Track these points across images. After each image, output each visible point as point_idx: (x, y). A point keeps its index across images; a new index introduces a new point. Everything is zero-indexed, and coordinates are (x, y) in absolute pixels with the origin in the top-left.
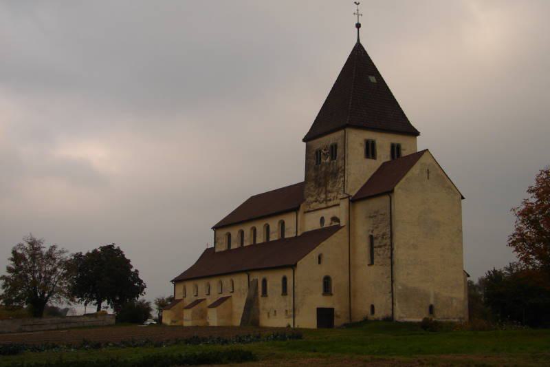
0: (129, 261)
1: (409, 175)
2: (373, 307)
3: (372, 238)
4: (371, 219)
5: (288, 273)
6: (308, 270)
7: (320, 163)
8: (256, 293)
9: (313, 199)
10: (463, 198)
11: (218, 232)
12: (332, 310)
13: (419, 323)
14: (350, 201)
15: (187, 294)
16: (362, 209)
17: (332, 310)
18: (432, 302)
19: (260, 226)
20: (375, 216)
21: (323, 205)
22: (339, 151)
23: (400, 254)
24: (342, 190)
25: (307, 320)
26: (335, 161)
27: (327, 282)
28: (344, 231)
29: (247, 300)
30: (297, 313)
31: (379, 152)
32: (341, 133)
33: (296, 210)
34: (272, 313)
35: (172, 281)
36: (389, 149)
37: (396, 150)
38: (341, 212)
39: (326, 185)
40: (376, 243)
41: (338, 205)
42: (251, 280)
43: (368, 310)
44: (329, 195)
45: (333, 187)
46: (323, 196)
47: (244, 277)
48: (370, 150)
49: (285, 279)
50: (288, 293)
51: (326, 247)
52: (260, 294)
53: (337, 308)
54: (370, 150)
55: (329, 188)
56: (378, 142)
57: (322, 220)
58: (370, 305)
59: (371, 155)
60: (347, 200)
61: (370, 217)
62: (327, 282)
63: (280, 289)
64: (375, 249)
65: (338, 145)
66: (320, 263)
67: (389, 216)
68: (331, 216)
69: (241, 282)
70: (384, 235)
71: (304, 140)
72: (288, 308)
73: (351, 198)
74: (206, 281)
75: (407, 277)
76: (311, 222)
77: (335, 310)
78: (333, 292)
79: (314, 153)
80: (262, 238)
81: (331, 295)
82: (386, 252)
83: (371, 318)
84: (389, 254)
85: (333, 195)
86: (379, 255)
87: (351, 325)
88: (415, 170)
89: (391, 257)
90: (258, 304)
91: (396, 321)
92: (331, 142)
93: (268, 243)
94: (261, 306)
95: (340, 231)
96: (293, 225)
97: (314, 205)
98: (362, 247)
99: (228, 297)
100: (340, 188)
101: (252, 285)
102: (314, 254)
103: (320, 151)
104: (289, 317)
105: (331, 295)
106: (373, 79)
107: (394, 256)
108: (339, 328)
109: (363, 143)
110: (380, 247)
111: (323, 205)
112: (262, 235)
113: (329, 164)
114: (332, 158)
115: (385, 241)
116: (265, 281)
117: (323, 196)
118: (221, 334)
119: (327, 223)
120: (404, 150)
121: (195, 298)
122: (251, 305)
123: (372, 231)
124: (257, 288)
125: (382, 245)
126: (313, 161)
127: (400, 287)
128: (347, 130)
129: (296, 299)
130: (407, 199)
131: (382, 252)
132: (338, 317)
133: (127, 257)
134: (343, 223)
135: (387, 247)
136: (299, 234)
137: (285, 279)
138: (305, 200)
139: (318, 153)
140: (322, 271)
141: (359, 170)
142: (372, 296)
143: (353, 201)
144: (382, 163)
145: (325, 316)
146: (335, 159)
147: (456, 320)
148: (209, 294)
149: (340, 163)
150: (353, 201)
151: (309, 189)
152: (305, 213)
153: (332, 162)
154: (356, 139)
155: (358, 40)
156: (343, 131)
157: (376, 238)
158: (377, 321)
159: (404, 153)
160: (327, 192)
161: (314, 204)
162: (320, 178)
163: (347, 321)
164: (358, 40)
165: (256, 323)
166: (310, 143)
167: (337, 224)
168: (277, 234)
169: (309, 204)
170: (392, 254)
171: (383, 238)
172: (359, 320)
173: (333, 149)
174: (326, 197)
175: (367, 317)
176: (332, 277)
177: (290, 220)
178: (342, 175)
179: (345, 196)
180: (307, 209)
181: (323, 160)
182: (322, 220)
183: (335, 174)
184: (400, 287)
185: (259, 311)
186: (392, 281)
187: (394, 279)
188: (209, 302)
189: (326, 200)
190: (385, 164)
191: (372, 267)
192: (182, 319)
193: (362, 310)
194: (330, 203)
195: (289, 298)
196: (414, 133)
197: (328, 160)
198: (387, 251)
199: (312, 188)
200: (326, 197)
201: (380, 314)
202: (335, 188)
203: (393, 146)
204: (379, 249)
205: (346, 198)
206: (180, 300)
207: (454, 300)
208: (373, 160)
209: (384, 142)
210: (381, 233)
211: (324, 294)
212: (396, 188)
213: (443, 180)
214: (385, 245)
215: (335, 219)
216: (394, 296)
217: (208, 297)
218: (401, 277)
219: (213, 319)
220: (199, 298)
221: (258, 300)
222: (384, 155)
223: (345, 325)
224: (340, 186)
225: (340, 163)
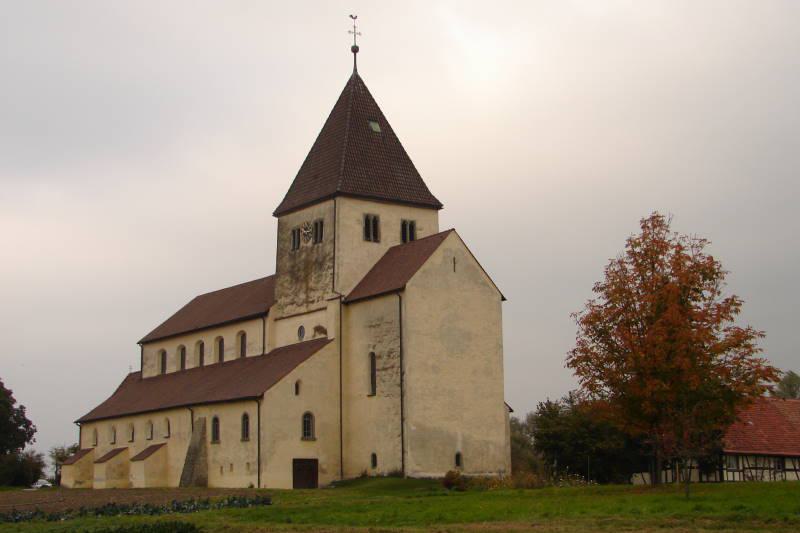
0: (10, 392)
1: (427, 266)
2: (374, 457)
3: (373, 356)
4: (373, 330)
5: (251, 409)
6: (281, 405)
7: (298, 248)
8: (203, 439)
9: (288, 300)
10: (503, 299)
11: (148, 348)
12: (315, 461)
13: (440, 479)
14: (342, 303)
15: (99, 440)
16: (357, 313)
17: (315, 461)
18: (459, 448)
19: (209, 340)
20: (379, 325)
21: (303, 309)
22: (327, 230)
23: (411, 378)
24: (331, 286)
25: (279, 477)
26: (320, 245)
27: (308, 421)
28: (333, 347)
29: (190, 447)
30: (263, 466)
31: (384, 232)
32: (329, 204)
34: (226, 469)
35: (76, 422)
36: (398, 228)
37: (408, 229)
38: (328, 318)
39: (306, 279)
40: (379, 364)
41: (325, 309)
42: (196, 419)
43: (368, 462)
44: (312, 294)
45: (318, 282)
46: (302, 296)
48: (371, 229)
49: (246, 418)
50: (251, 437)
51: (305, 371)
52: (209, 438)
53: (322, 460)
54: (371, 229)
55: (312, 284)
56: (382, 220)
57: (301, 331)
58: (370, 455)
59: (372, 237)
60: (338, 300)
61: (370, 326)
62: (308, 421)
63: (239, 434)
64: (377, 373)
66: (297, 393)
67: (398, 323)
68: (315, 324)
69: (181, 421)
71: (276, 214)
72: (250, 460)
73: (343, 299)
75: (424, 412)
76: (285, 335)
77: (320, 462)
78: (316, 436)
79: (290, 232)
80: (212, 357)
81: (314, 439)
82: (394, 377)
83: (372, 472)
84: (398, 381)
85: (318, 294)
86: (384, 381)
87: (343, 484)
88: (437, 258)
89: (401, 385)
90: (206, 455)
91: (408, 477)
92: (315, 218)
93: (221, 364)
94: (210, 457)
95: (327, 347)
96: (258, 339)
97: (290, 310)
98: (360, 369)
99: (162, 445)
100: (327, 285)
101: (197, 427)
102: (289, 381)
103: (299, 230)
104: (251, 474)
105: (314, 439)
106: (376, 127)
107: (404, 383)
108: (323, 488)
109: (362, 219)
110: (385, 369)
111: (303, 309)
112: (213, 352)
113: (312, 248)
114: (316, 242)
116: (216, 421)
117: (302, 296)
118: (151, 500)
119: (309, 335)
120: (421, 230)
121: (113, 447)
122: (195, 456)
123: (374, 347)
124: (204, 428)
125: (386, 368)
126: (289, 245)
127: (413, 428)
128: (339, 200)
129: (261, 446)
130: (425, 297)
131: (387, 377)
132: (324, 472)
133: (7, 386)
134: (332, 334)
135: (395, 369)
136: (267, 352)
137: (246, 418)
138: (276, 301)
139: (296, 233)
140: (300, 406)
141: (354, 258)
142: (373, 440)
143: (347, 303)
144: (388, 248)
145: (305, 471)
146: (321, 241)
147: (494, 474)
148: (132, 441)
150: (347, 303)
151: (282, 285)
152: (276, 320)
153: (316, 246)
154: (351, 214)
155: (355, 70)
156: (332, 202)
157: (380, 357)
158: (380, 477)
159: (420, 234)
160: (308, 290)
161: (290, 307)
162: (299, 270)
163: (338, 478)
164: (355, 70)
165: (203, 483)
166: (285, 218)
167: (323, 336)
168: (233, 352)
169: (282, 307)
170: (402, 380)
171: (389, 356)
172: (354, 476)
174: (308, 297)
175: (366, 472)
176: (315, 415)
177: (254, 330)
179: (335, 296)
180: (279, 315)
181: (302, 244)
182: (301, 331)
183: (320, 264)
184: (413, 428)
185: (207, 465)
186: (403, 420)
187: (405, 416)
188: (133, 452)
189: (308, 302)
190: (393, 250)
191: (374, 399)
192: (91, 478)
193: (359, 463)
194: (313, 307)
195: (253, 444)
196: (436, 206)
197: (310, 244)
198: (395, 376)
199: (286, 284)
201: (385, 466)
202: (320, 285)
203: (404, 224)
204: (384, 373)
205: (336, 298)
206: (89, 451)
207: (491, 446)
208: (376, 245)
209: (391, 218)
210: (387, 350)
211: (302, 439)
212: (408, 285)
213: (476, 273)
214: (393, 367)
215: (319, 329)
216: (405, 442)
217: (131, 446)
218: (415, 414)
219: (139, 477)
220: (119, 447)
221: (206, 447)
222: (391, 237)
223: (334, 483)
224: (328, 280)
225: (328, 248)
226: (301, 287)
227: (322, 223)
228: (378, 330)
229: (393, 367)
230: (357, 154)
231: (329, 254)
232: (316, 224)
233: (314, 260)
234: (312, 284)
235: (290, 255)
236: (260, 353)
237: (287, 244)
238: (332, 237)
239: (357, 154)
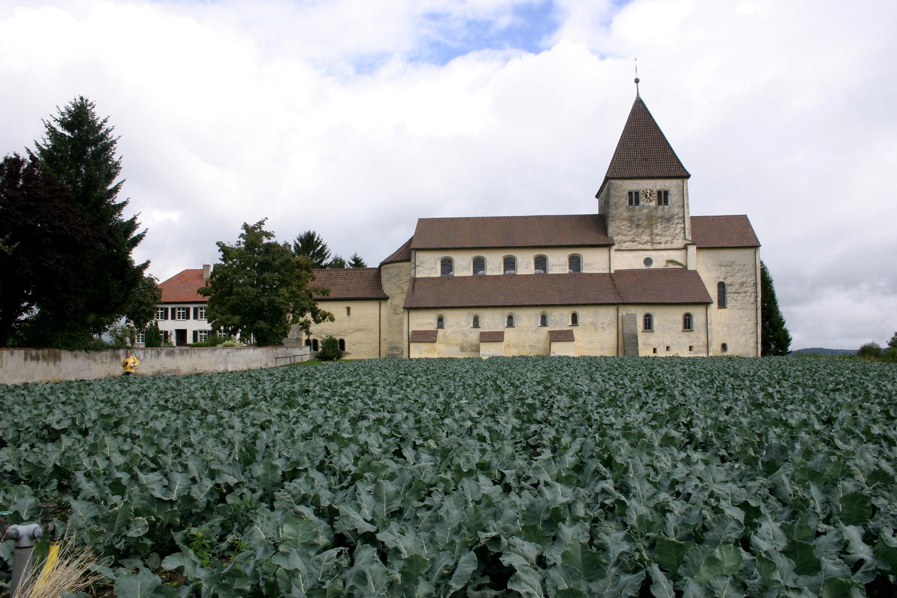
4: (723, 268)
22: (673, 198)
24: (682, 235)
33: (608, 246)
39: (650, 226)
40: (729, 289)
44: (658, 238)
47: (607, 315)
55: (655, 231)
57: (648, 261)
65: (671, 192)
70: (742, 284)
74: (507, 312)
84: (752, 300)
85: (663, 239)
92: (658, 188)
113: (656, 209)
114: (660, 203)
115: (744, 289)
117: (645, 238)
123: (725, 278)
146: (666, 203)
149: (676, 210)
157: (731, 285)
162: (639, 220)
173: (663, 197)
181: (642, 203)
182: (648, 261)
183: (669, 220)
194: (659, 247)
202: (668, 233)
214: (746, 292)
227: (666, 193)
228: (729, 269)
229: (746, 292)
231: (677, 214)
232: (659, 193)
234: (655, 231)
235: (628, 208)
236: (607, 271)
237: (623, 200)
238: (681, 204)
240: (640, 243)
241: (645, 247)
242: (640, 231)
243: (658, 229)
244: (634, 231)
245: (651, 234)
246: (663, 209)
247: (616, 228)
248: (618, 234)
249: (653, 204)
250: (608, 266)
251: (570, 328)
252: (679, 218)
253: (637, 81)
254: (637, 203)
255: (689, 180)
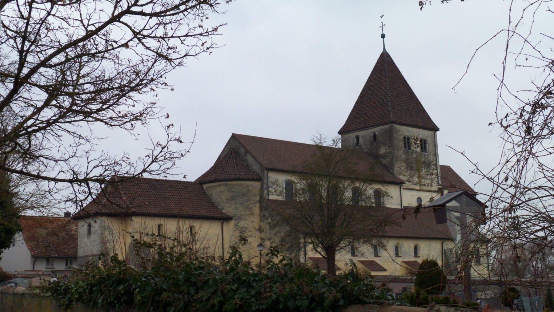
21: (417, 187)
39: (418, 170)
44: (423, 180)
57: (419, 199)
79: (402, 137)
92: (421, 136)
111: (417, 187)
113: (420, 154)
117: (416, 179)
146: (426, 151)
149: (432, 158)
162: (412, 163)
178: (435, 168)
182: (419, 199)
189: (419, 183)
194: (424, 188)
199: (403, 168)
200: (420, 181)
226: (414, 173)
230: (387, 99)
233: (422, 160)
235: (404, 151)
238: (434, 153)
239: (387, 99)
240: (413, 183)
241: (413, 187)
242: (413, 173)
243: (423, 172)
244: (409, 173)
245: (419, 177)
246: (425, 155)
247: (400, 170)
248: (400, 174)
249: (418, 149)
250: (400, 202)
251: (414, 259)
252: (434, 165)
253: (383, 36)
254: (409, 148)
255: (437, 132)
